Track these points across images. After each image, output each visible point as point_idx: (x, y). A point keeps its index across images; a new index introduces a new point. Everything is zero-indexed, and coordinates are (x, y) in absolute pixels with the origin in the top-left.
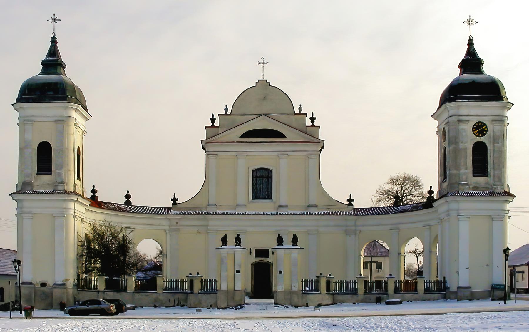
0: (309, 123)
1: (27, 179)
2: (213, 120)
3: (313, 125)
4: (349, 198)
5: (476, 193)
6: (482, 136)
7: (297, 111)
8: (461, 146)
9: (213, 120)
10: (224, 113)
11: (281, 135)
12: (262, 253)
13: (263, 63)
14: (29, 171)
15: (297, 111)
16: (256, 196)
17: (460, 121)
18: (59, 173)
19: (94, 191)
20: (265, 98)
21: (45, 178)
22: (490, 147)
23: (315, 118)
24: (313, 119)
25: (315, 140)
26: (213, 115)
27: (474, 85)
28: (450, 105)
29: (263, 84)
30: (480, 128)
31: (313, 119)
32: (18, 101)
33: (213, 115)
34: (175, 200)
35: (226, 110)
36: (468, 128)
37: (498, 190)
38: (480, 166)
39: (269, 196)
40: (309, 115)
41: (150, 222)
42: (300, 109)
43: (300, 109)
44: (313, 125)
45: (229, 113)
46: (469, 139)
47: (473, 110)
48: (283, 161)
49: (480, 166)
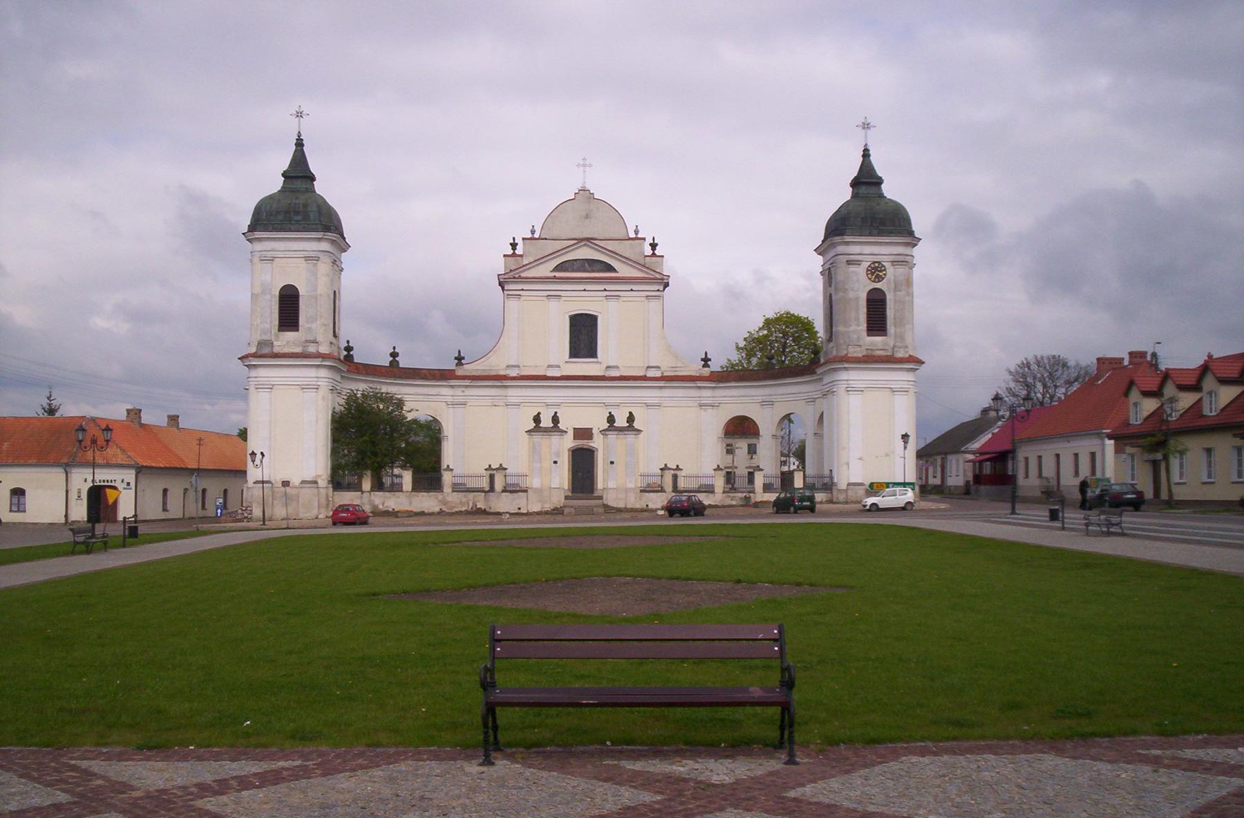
0: (648, 251)
1: (265, 337)
2: (514, 246)
3: (654, 255)
5: (870, 360)
8: (851, 295)
9: (514, 246)
11: (610, 268)
12: (583, 433)
13: (584, 165)
14: (267, 326)
15: (632, 235)
16: (575, 352)
17: (849, 262)
18: (309, 329)
19: (349, 349)
20: (587, 217)
21: (290, 335)
22: (889, 297)
24: (654, 246)
25: (658, 276)
27: (869, 212)
28: (838, 239)
29: (585, 194)
30: (876, 271)
31: (654, 246)
32: (252, 228)
34: (459, 359)
35: (533, 232)
36: (861, 270)
37: (900, 354)
38: (877, 320)
39: (591, 352)
41: (425, 390)
42: (636, 232)
43: (636, 232)
44: (654, 255)
46: (859, 286)
47: (867, 250)
48: (612, 304)
49: (877, 320)
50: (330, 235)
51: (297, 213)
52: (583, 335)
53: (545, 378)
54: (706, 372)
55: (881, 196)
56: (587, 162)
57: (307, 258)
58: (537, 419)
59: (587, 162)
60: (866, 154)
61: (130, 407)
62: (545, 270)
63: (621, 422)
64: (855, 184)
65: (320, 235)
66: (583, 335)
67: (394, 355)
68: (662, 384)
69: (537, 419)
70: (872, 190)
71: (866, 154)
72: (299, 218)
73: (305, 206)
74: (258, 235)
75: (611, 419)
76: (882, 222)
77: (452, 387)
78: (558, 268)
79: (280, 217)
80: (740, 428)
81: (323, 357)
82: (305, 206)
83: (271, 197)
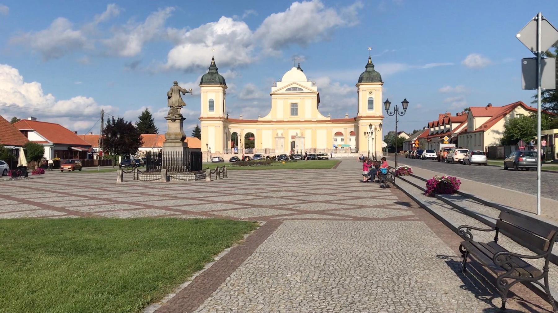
12: (293, 137)
32: (201, 83)
39: (296, 114)
50: (222, 85)
52: (294, 109)
53: (283, 122)
58: (277, 135)
62: (283, 91)
66: (294, 109)
70: (372, 68)
74: (202, 85)
76: (372, 79)
78: (287, 90)
81: (221, 118)
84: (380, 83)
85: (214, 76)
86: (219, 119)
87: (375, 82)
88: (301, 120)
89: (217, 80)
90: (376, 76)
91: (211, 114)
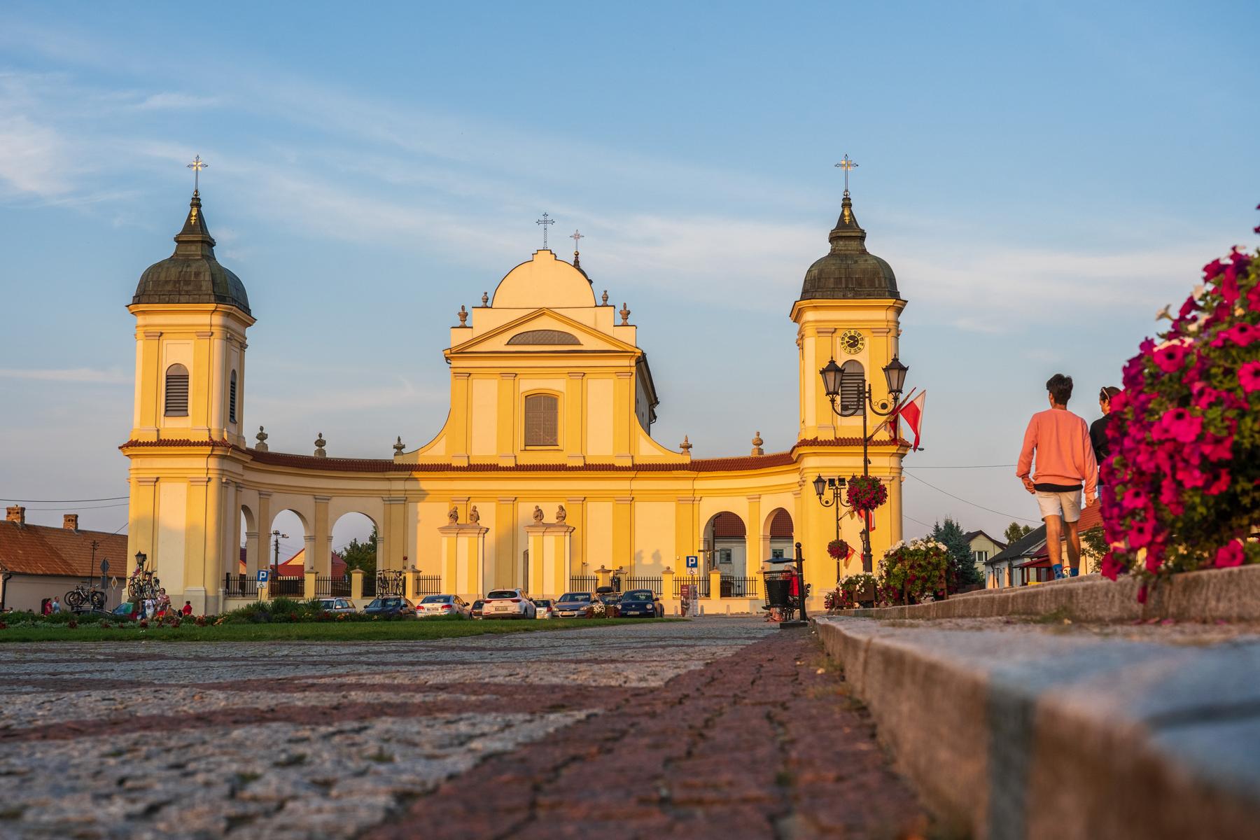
4: (683, 442)
6: (856, 352)
7: (601, 302)
9: (464, 316)
10: (482, 304)
23: (629, 313)
26: (463, 308)
33: (463, 308)
40: (620, 307)
43: (605, 298)
45: (489, 304)
50: (222, 307)
51: (187, 283)
52: (541, 417)
54: (686, 460)
55: (864, 252)
56: (549, 218)
57: (200, 335)
59: (549, 218)
60: (847, 203)
61: (12, 505)
62: (499, 344)
63: (550, 517)
64: (833, 238)
65: (212, 307)
66: (541, 417)
67: (320, 443)
68: (632, 474)
69: (454, 516)
71: (847, 203)
72: (190, 288)
73: (197, 274)
74: (142, 307)
75: (539, 514)
76: (860, 283)
77: (389, 479)
79: (169, 287)
80: (726, 528)
81: (212, 444)
82: (197, 274)
83: (159, 266)
84: (891, 302)
85: (193, 269)
86: (208, 450)
87: (869, 296)
88: (570, 464)
89: (206, 285)
90: (875, 273)
91: (175, 427)
